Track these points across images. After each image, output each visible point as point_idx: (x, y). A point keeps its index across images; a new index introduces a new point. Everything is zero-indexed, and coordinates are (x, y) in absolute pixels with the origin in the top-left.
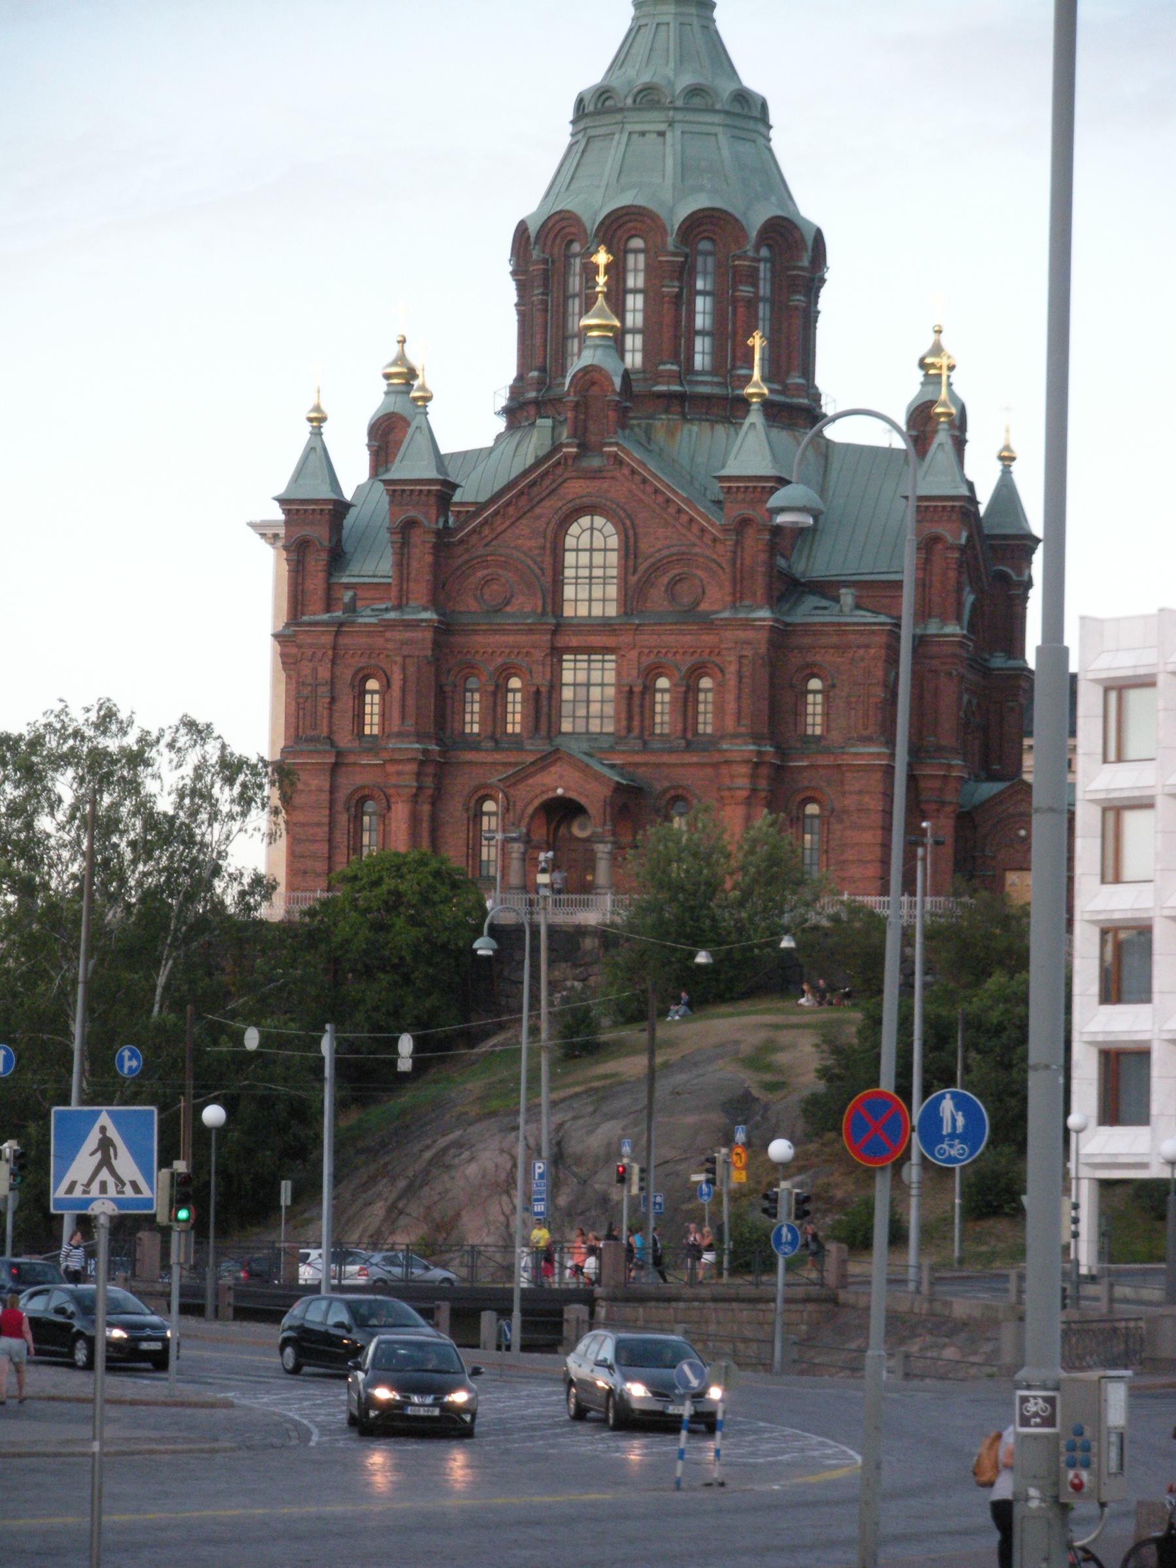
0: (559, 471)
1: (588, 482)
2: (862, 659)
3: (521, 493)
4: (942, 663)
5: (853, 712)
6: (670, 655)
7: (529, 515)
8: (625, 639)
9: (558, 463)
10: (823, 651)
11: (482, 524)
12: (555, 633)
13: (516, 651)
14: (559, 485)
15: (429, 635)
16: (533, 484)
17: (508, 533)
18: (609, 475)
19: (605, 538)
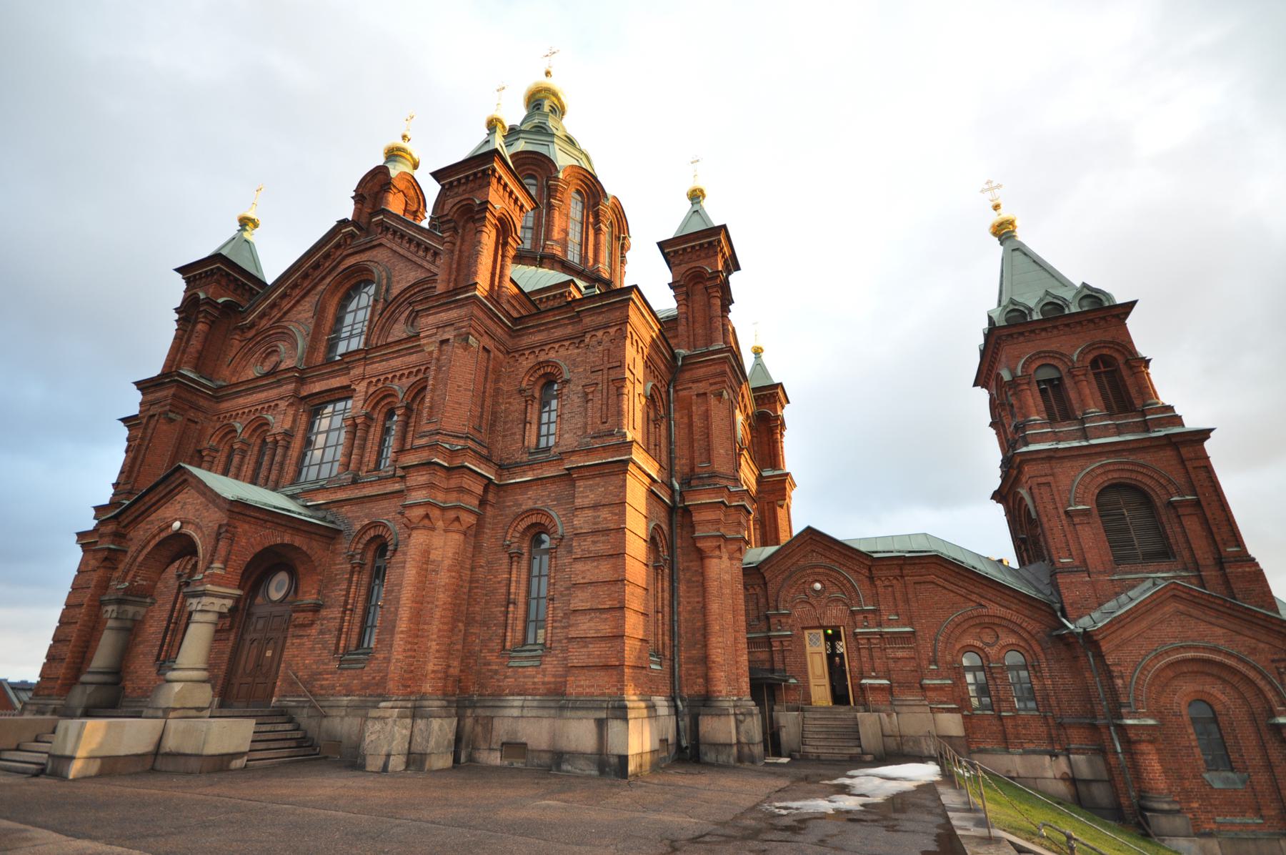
0: (338, 253)
1: (362, 255)
2: (600, 343)
3: (305, 276)
4: (711, 384)
5: (590, 404)
6: (396, 380)
7: (313, 292)
8: (356, 372)
9: (338, 246)
10: (557, 346)
11: (273, 306)
12: (301, 381)
13: (266, 406)
14: (339, 263)
15: (172, 391)
16: (316, 266)
17: (294, 311)
18: (375, 243)
19: (369, 297)
